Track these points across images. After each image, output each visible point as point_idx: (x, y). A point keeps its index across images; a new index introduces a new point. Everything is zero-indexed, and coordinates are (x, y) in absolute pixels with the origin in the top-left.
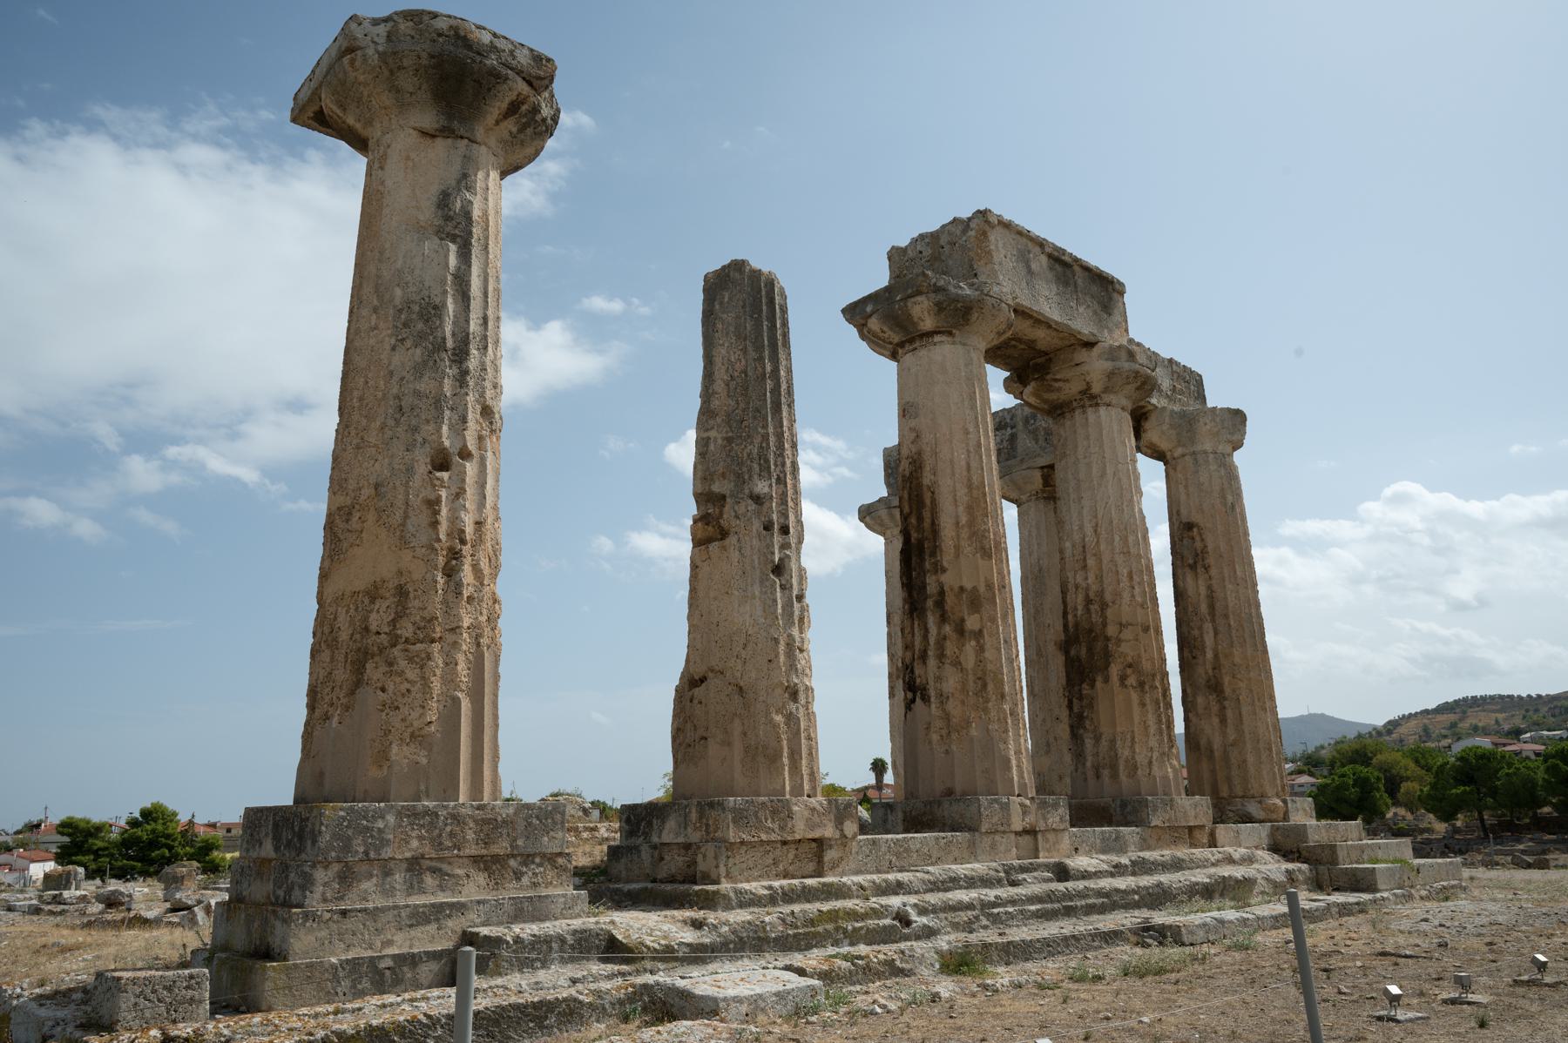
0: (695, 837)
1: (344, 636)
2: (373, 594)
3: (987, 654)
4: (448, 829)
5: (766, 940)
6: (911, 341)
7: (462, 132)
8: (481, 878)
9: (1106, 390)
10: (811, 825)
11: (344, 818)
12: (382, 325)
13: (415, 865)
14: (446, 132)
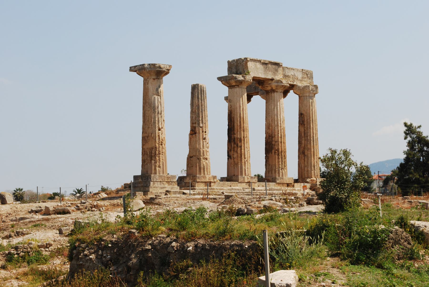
1: (149, 153)
8: (167, 184)
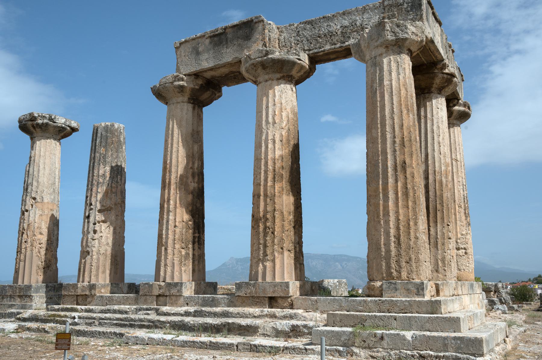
5: (38, 319)
10: (83, 291)
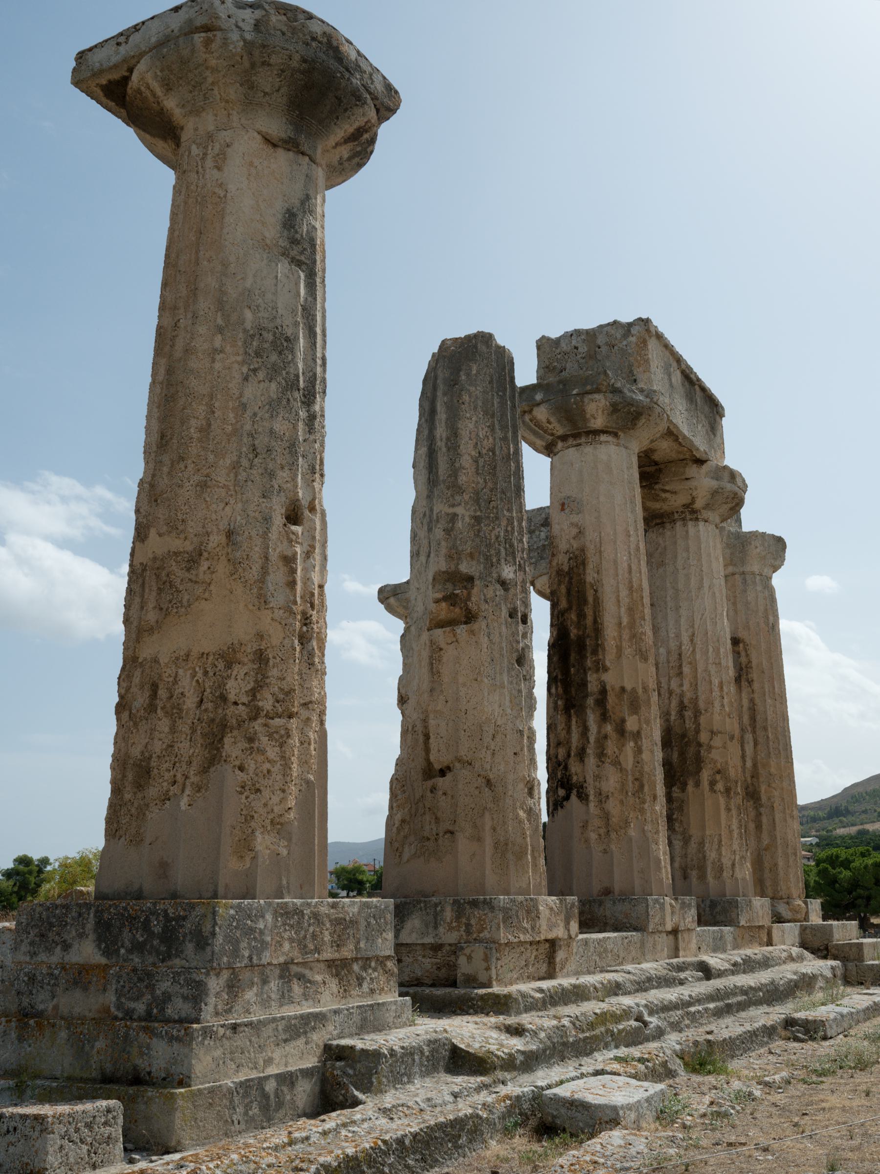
0: (450, 938)
2: (229, 658)
3: (644, 756)
4: (311, 929)
6: (576, 436)
7: (305, 148)
8: (333, 985)
9: (707, 507)
11: (233, 917)
12: (228, 349)
13: (285, 971)
14: (291, 145)
